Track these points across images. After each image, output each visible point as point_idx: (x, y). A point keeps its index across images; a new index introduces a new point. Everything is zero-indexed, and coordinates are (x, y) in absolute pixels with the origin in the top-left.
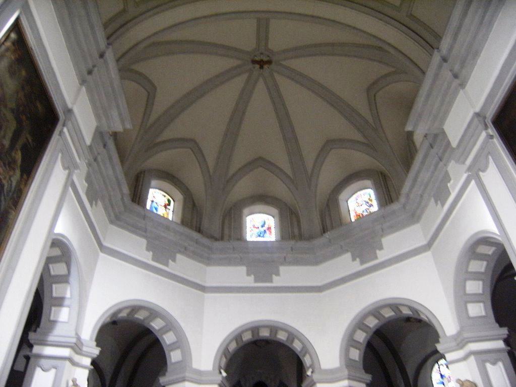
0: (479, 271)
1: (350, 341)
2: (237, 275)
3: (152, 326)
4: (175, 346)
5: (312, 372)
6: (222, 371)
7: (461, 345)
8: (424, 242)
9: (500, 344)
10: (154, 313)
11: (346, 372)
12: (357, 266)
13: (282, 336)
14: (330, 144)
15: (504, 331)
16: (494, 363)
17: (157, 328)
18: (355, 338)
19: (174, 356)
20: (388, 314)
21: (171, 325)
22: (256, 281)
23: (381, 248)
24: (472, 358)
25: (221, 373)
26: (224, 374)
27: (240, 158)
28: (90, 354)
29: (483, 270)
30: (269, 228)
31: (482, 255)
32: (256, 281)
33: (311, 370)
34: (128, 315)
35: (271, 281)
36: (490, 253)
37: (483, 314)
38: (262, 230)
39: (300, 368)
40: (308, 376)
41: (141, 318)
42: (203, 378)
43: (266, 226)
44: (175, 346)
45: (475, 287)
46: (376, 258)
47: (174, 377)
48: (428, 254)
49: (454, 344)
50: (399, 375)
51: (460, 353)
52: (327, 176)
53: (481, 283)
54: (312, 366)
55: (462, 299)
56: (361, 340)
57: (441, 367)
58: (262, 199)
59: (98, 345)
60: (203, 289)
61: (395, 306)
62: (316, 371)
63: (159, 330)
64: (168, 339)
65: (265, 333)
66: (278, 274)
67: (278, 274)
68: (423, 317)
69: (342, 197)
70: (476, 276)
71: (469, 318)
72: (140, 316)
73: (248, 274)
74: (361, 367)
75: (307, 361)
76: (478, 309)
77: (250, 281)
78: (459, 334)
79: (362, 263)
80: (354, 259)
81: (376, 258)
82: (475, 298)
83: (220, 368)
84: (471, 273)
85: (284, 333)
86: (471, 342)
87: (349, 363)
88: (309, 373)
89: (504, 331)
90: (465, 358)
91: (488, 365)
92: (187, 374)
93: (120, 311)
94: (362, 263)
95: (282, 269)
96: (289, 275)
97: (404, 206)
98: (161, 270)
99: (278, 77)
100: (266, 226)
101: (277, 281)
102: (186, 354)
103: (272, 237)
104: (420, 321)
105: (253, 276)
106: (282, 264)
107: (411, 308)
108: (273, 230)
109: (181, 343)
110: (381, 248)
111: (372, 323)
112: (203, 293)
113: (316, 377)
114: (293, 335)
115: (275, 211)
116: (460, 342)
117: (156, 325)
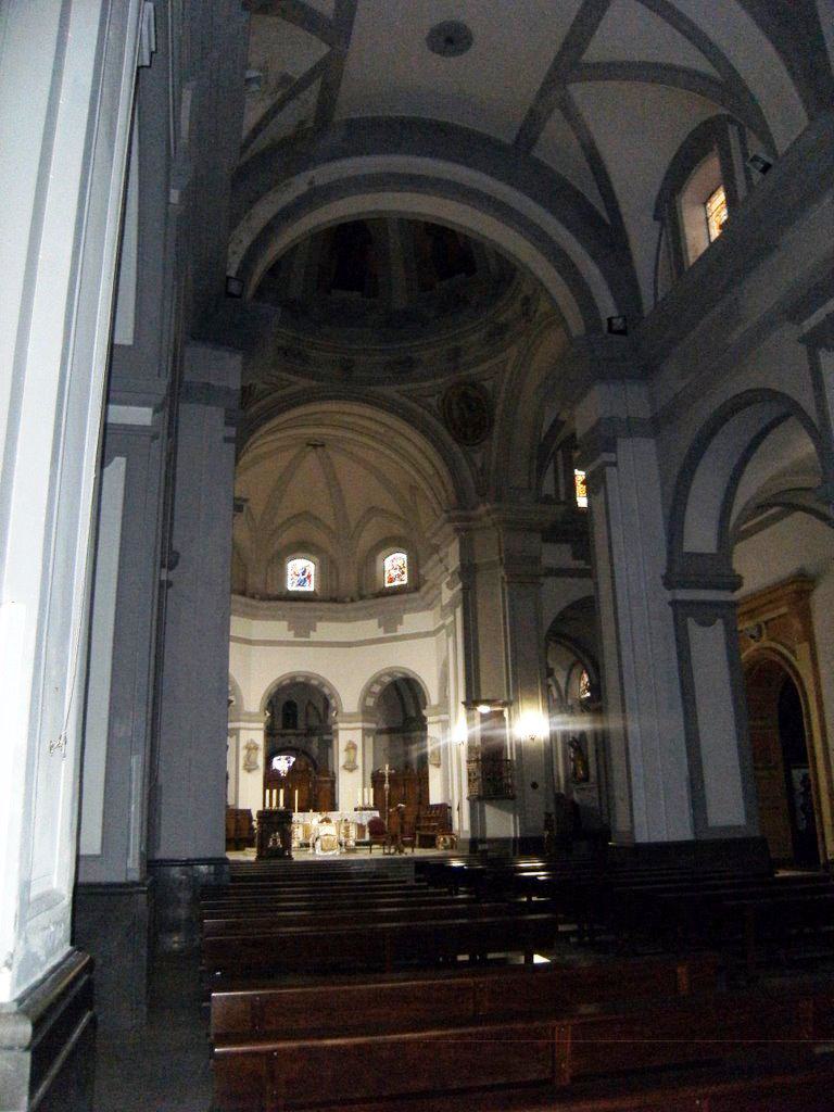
1: (368, 692)
2: (278, 629)
8: (433, 629)
14: (372, 511)
26: (268, 714)
30: (309, 577)
32: (296, 635)
38: (302, 578)
39: (327, 705)
43: (307, 574)
46: (396, 631)
52: (367, 539)
54: (336, 709)
56: (371, 704)
58: (302, 547)
62: (339, 714)
66: (315, 631)
67: (315, 631)
73: (289, 630)
75: (333, 702)
77: (290, 636)
81: (396, 631)
96: (326, 630)
97: (423, 598)
100: (307, 574)
101: (314, 636)
103: (310, 587)
108: (312, 577)
113: (338, 719)
114: (323, 683)
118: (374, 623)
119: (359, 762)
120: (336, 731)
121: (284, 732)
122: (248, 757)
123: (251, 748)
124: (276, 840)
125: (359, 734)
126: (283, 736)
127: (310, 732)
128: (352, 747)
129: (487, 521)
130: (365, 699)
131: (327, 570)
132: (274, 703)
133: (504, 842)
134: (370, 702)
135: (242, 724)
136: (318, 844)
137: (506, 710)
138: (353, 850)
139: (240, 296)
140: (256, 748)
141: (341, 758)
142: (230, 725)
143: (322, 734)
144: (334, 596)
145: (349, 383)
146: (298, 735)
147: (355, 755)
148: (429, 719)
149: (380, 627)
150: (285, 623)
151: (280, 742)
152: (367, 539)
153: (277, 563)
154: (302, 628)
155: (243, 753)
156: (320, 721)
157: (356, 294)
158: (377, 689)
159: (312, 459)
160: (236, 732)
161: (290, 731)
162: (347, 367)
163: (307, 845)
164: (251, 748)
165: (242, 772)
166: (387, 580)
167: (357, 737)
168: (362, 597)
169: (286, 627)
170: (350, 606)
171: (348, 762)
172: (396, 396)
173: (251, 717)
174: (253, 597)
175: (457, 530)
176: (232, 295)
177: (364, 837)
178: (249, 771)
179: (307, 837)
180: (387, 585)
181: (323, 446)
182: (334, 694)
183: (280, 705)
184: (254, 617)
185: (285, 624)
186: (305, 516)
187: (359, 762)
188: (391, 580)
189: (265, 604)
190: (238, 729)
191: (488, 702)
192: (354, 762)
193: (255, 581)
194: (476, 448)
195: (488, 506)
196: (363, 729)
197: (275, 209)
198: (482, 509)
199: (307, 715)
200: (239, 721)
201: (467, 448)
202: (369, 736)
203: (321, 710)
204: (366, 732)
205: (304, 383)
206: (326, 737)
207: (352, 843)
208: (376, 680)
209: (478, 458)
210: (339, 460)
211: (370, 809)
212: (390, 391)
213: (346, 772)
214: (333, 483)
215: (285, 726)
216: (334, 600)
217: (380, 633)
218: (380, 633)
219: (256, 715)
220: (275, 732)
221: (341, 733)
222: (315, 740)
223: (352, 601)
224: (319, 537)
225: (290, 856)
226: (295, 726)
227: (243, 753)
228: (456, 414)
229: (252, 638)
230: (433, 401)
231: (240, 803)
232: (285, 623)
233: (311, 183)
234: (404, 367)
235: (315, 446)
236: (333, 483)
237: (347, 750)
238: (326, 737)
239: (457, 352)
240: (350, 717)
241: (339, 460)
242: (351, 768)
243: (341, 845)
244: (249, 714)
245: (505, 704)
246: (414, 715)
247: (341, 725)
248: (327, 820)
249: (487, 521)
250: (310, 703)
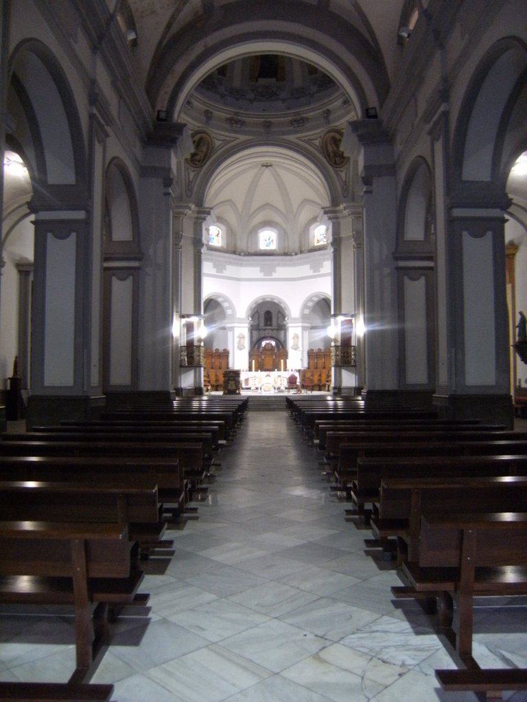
1: (305, 306)
19: (229, 312)
21: (227, 300)
23: (322, 267)
27: (256, 204)
30: (272, 241)
38: (268, 242)
44: (228, 308)
52: (304, 216)
58: (267, 224)
60: (238, 280)
67: (275, 272)
69: (311, 228)
73: (261, 272)
77: (261, 275)
94: (314, 272)
95: (277, 268)
96: (282, 271)
98: (221, 276)
99: (278, 170)
101: (275, 275)
102: (234, 311)
109: (232, 307)
110: (322, 267)
115: (276, 231)
118: (308, 267)
119: (300, 345)
124: (231, 386)
125: (300, 329)
126: (264, 330)
128: (296, 337)
129: (346, 212)
130: (303, 311)
131: (283, 236)
133: (350, 388)
135: (235, 325)
137: (353, 319)
138: (282, 391)
139: (166, 120)
144: (286, 251)
145: (268, 135)
146: (272, 330)
147: (298, 341)
148: (290, 325)
151: (263, 334)
152: (304, 216)
153: (254, 232)
154: (268, 271)
157: (273, 80)
158: (310, 304)
159: (267, 171)
160: (232, 329)
161: (268, 327)
162: (268, 125)
165: (237, 351)
166: (316, 241)
167: (299, 331)
168: (301, 252)
170: (294, 257)
172: (296, 141)
173: (240, 321)
174: (240, 255)
175: (330, 219)
176: (163, 120)
178: (240, 349)
180: (316, 244)
181: (271, 166)
183: (262, 313)
184: (241, 265)
185: (258, 268)
186: (267, 205)
187: (300, 345)
188: (318, 241)
189: (246, 258)
190: (234, 327)
191: (345, 315)
193: (242, 245)
194: (342, 169)
195: (345, 205)
196: (302, 327)
197: (187, 64)
198: (342, 207)
199: (278, 318)
200: (234, 323)
201: (338, 169)
202: (306, 330)
204: (304, 328)
205: (242, 138)
207: (283, 388)
208: (310, 299)
209: (343, 175)
210: (282, 172)
212: (292, 138)
213: (293, 350)
214: (281, 185)
215: (266, 325)
216: (286, 254)
217: (311, 273)
221: (290, 329)
223: (296, 254)
224: (277, 218)
225: (239, 394)
227: (237, 340)
228: (330, 149)
230: (317, 142)
231: (235, 365)
232: (258, 268)
233: (205, 46)
234: (299, 123)
235: (267, 166)
236: (281, 185)
237: (293, 338)
239: (328, 112)
240: (295, 320)
241: (282, 172)
242: (296, 348)
243: (275, 388)
245: (352, 316)
248: (268, 375)
249: (346, 212)
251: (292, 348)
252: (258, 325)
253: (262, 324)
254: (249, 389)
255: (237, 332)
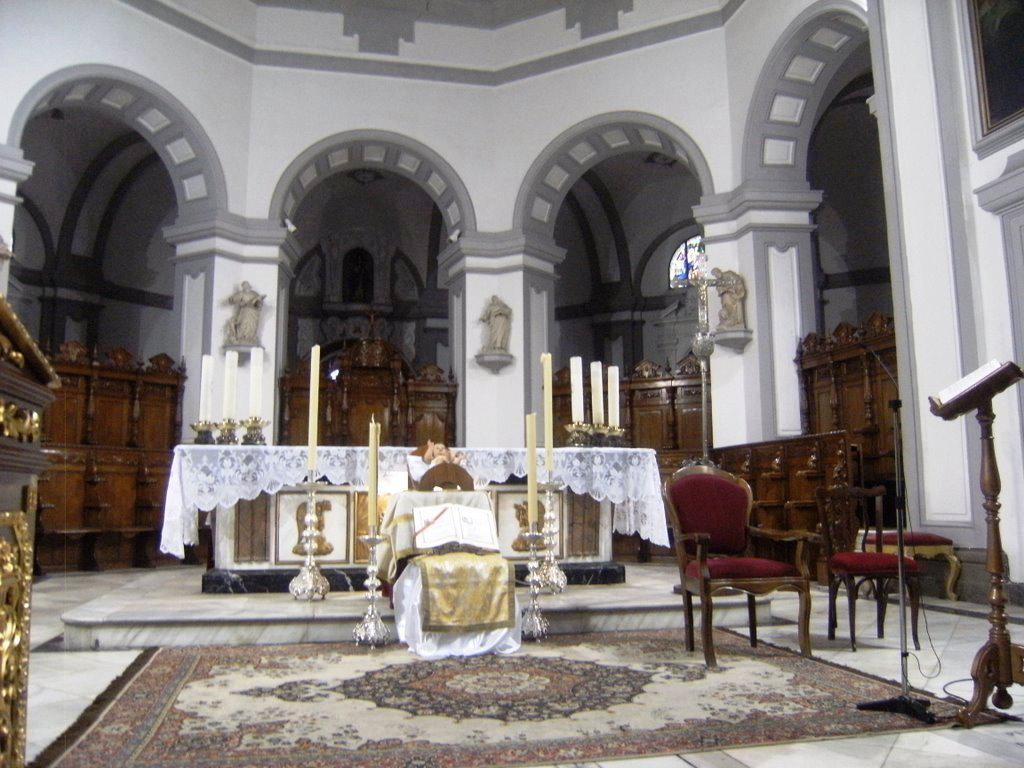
0: (805, 79)
1: (536, 185)
3: (140, 125)
4: (192, 168)
5: (459, 236)
6: (288, 221)
7: (734, 214)
8: (717, 8)
9: (802, 218)
10: (145, 96)
11: (522, 241)
12: (573, 40)
13: (407, 165)
15: (817, 197)
16: (783, 249)
17: (153, 130)
18: (547, 181)
19: (192, 188)
20: (617, 141)
21: (181, 125)
22: (362, 48)
24: (749, 236)
25: (285, 225)
26: (292, 228)
28: (16, 175)
29: (812, 79)
31: (817, 46)
32: (362, 48)
33: (457, 232)
34: (88, 97)
35: (395, 52)
36: (836, 46)
37: (790, 161)
39: (436, 223)
40: (451, 241)
41: (119, 106)
42: (251, 233)
44: (192, 168)
45: (788, 109)
46: (615, 27)
47: (191, 229)
48: (720, 31)
49: (723, 208)
50: (613, 254)
51: (731, 226)
53: (802, 103)
54: (460, 225)
55: (759, 128)
57: (690, 251)
59: (26, 157)
61: (631, 126)
63: (158, 133)
64: (178, 152)
65: (374, 157)
66: (410, 38)
67: (410, 38)
68: (680, 154)
70: (796, 89)
71: (763, 165)
72: (115, 101)
73: (347, 32)
74: (551, 234)
75: (452, 214)
76: (780, 152)
77: (348, 47)
78: (737, 192)
79: (585, 35)
80: (569, 25)
81: (615, 27)
82: (783, 131)
83: (283, 216)
84: (792, 81)
85: (413, 159)
86: (754, 208)
87: (528, 224)
88: (454, 237)
89: (817, 197)
90: (736, 236)
91: (773, 251)
92: (218, 223)
93: (68, 87)
94: (585, 35)
95: (421, 28)
101: (407, 53)
104: (672, 163)
105: (356, 36)
106: (420, 18)
107: (663, 136)
109: (204, 163)
111: (584, 155)
112: (248, 64)
113: (465, 244)
114: (430, 163)
116: (736, 205)
117: (151, 122)
120: (461, 275)
121: (343, 308)
122: (235, 326)
123: (246, 302)
125: (520, 274)
126: (344, 316)
127: (400, 313)
128: (497, 313)
132: (324, 249)
134: (544, 211)
135: (220, 244)
136: (410, 589)
140: (257, 304)
141: (473, 338)
142: (183, 249)
143: (420, 318)
147: (507, 332)
149: (569, 25)
150: (339, 18)
155: (221, 316)
156: (421, 291)
160: (204, 262)
163: (358, 580)
164: (246, 302)
167: (511, 289)
169: (341, 27)
171: (490, 346)
173: (244, 230)
177: (595, 550)
179: (362, 550)
182: (455, 191)
183: (337, 255)
190: (211, 254)
192: (504, 347)
196: (528, 271)
199: (394, 278)
203: (424, 276)
206: (432, 323)
211: (614, 441)
215: (348, 298)
218: (573, 40)
219: (258, 223)
220: (327, 307)
221: (471, 280)
222: (410, 328)
226: (367, 298)
227: (221, 316)
229: (257, 46)
232: (339, 18)
237: (486, 319)
238: (432, 323)
240: (495, 245)
242: (495, 363)
244: (242, 221)
246: (616, 277)
247: (470, 262)
248: (451, 478)
250: (399, 255)
251: (481, 361)
252: (320, 298)
253: (335, 294)
254: (276, 583)
255: (226, 277)
